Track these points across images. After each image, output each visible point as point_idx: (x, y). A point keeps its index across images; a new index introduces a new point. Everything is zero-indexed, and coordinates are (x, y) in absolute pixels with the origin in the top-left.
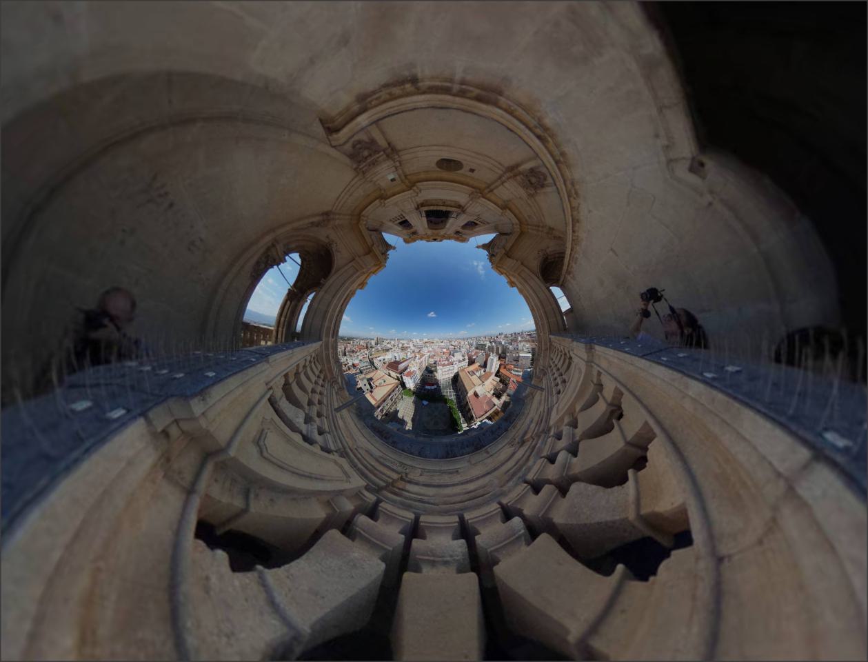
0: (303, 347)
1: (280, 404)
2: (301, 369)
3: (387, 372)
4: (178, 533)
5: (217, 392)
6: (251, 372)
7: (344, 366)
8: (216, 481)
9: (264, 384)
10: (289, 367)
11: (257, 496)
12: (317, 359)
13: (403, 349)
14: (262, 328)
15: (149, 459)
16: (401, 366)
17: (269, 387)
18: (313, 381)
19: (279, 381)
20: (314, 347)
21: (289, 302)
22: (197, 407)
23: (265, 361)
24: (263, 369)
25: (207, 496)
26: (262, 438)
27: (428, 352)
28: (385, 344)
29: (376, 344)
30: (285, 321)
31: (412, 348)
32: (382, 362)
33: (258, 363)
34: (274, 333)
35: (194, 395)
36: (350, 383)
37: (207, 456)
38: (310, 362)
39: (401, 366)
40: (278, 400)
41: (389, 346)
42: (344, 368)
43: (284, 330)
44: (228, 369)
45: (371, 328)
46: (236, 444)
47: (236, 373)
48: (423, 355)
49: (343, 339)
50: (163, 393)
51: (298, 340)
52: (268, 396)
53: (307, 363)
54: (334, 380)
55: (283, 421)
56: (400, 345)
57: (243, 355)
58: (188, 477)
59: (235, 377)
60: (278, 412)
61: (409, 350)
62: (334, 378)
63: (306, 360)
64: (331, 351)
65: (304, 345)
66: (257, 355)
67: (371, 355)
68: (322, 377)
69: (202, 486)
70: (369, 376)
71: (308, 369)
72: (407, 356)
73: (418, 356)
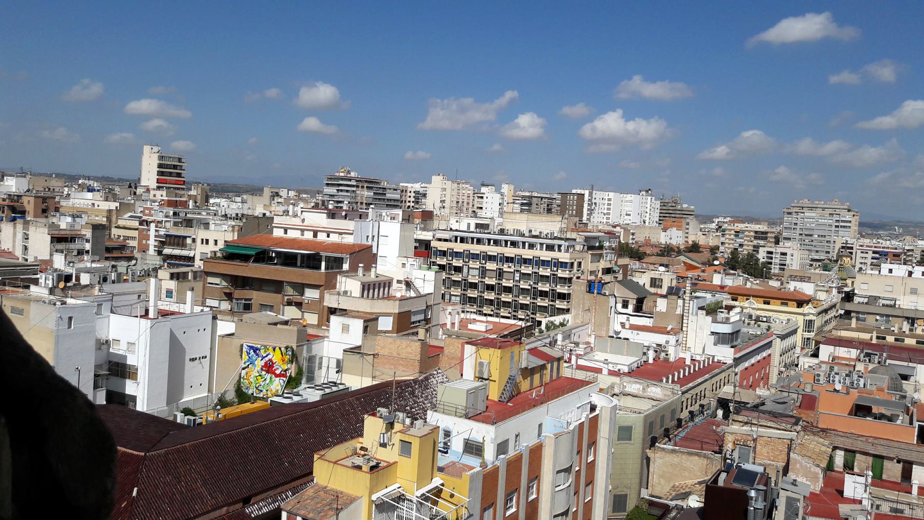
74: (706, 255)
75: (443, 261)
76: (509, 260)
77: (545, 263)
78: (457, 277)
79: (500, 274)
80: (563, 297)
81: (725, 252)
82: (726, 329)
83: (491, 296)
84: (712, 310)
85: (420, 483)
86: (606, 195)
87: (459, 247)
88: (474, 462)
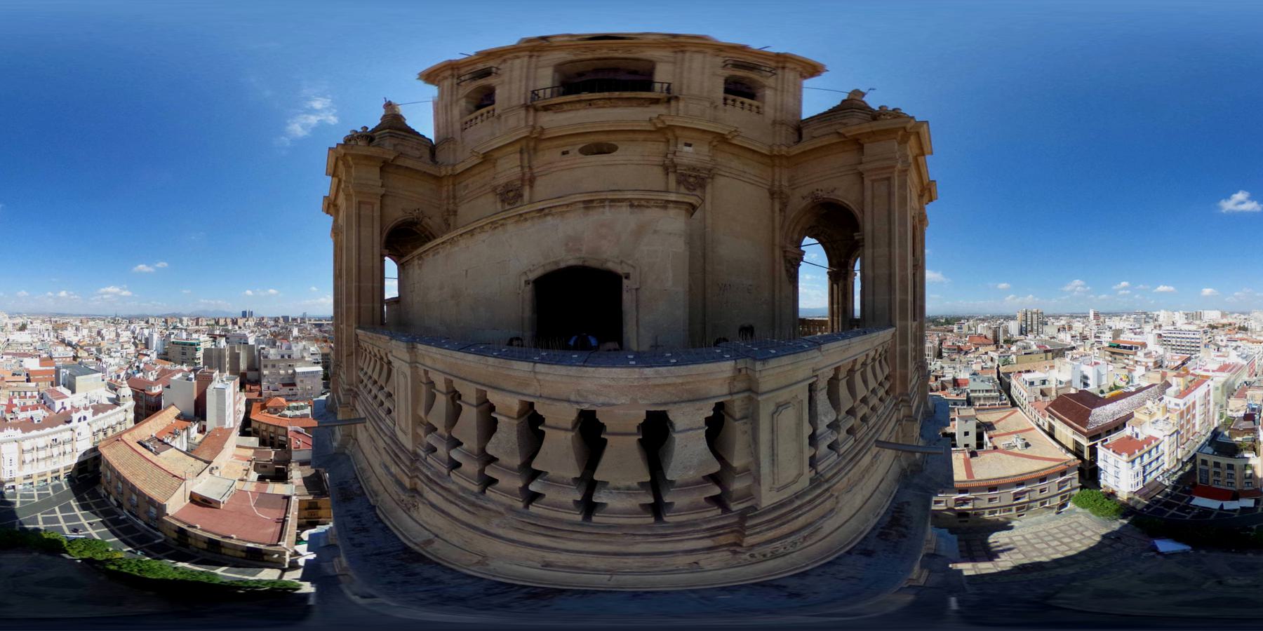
0: (864, 337)
1: (819, 394)
2: (858, 366)
3: (1046, 421)
4: (714, 397)
5: (773, 363)
6: (802, 356)
7: (933, 378)
8: (743, 401)
9: (811, 370)
10: (842, 361)
11: (746, 423)
12: (886, 356)
13: (1118, 350)
14: (817, 320)
15: (729, 374)
16: (1102, 415)
17: (815, 374)
18: (871, 389)
19: (827, 372)
20: (882, 337)
21: (835, 286)
22: (759, 366)
23: (818, 349)
24: (814, 356)
25: (733, 401)
26: (784, 407)
27: (1223, 369)
28: (1050, 330)
29: (1023, 331)
30: (838, 308)
31: (1154, 347)
32: (1038, 387)
33: (811, 350)
34: (830, 323)
35: (760, 360)
36: (936, 415)
37: (749, 390)
38: (874, 359)
39: (1102, 415)
40: (819, 389)
41: (1065, 338)
42: (933, 384)
43: (840, 318)
44: (784, 351)
45: (1003, 285)
46: (764, 397)
47: (790, 354)
48: (1199, 381)
49: (935, 321)
50: (746, 354)
51: (858, 328)
52: (810, 381)
53: (869, 360)
54: (905, 398)
55: (809, 410)
56: (1107, 338)
57: (798, 342)
58: (735, 390)
59: (789, 356)
60: (811, 400)
61: (1140, 354)
62: (908, 395)
63: (867, 355)
64: (911, 345)
65: (865, 333)
66: (810, 343)
67: (1006, 363)
68: (887, 386)
69: (735, 397)
70: (985, 418)
71: (869, 369)
72: (1130, 380)
73: (1177, 383)
74: (1233, 326)
75: (1165, 339)
76: (1183, 338)
77: (1193, 338)
78: (1169, 343)
79: (1181, 342)
80: (1198, 347)
81: (1237, 326)
82: (1240, 353)
83: (1179, 348)
84: (1235, 349)
85: (1163, 416)
86: (1207, 311)
87: (1169, 335)
88: (1177, 408)
